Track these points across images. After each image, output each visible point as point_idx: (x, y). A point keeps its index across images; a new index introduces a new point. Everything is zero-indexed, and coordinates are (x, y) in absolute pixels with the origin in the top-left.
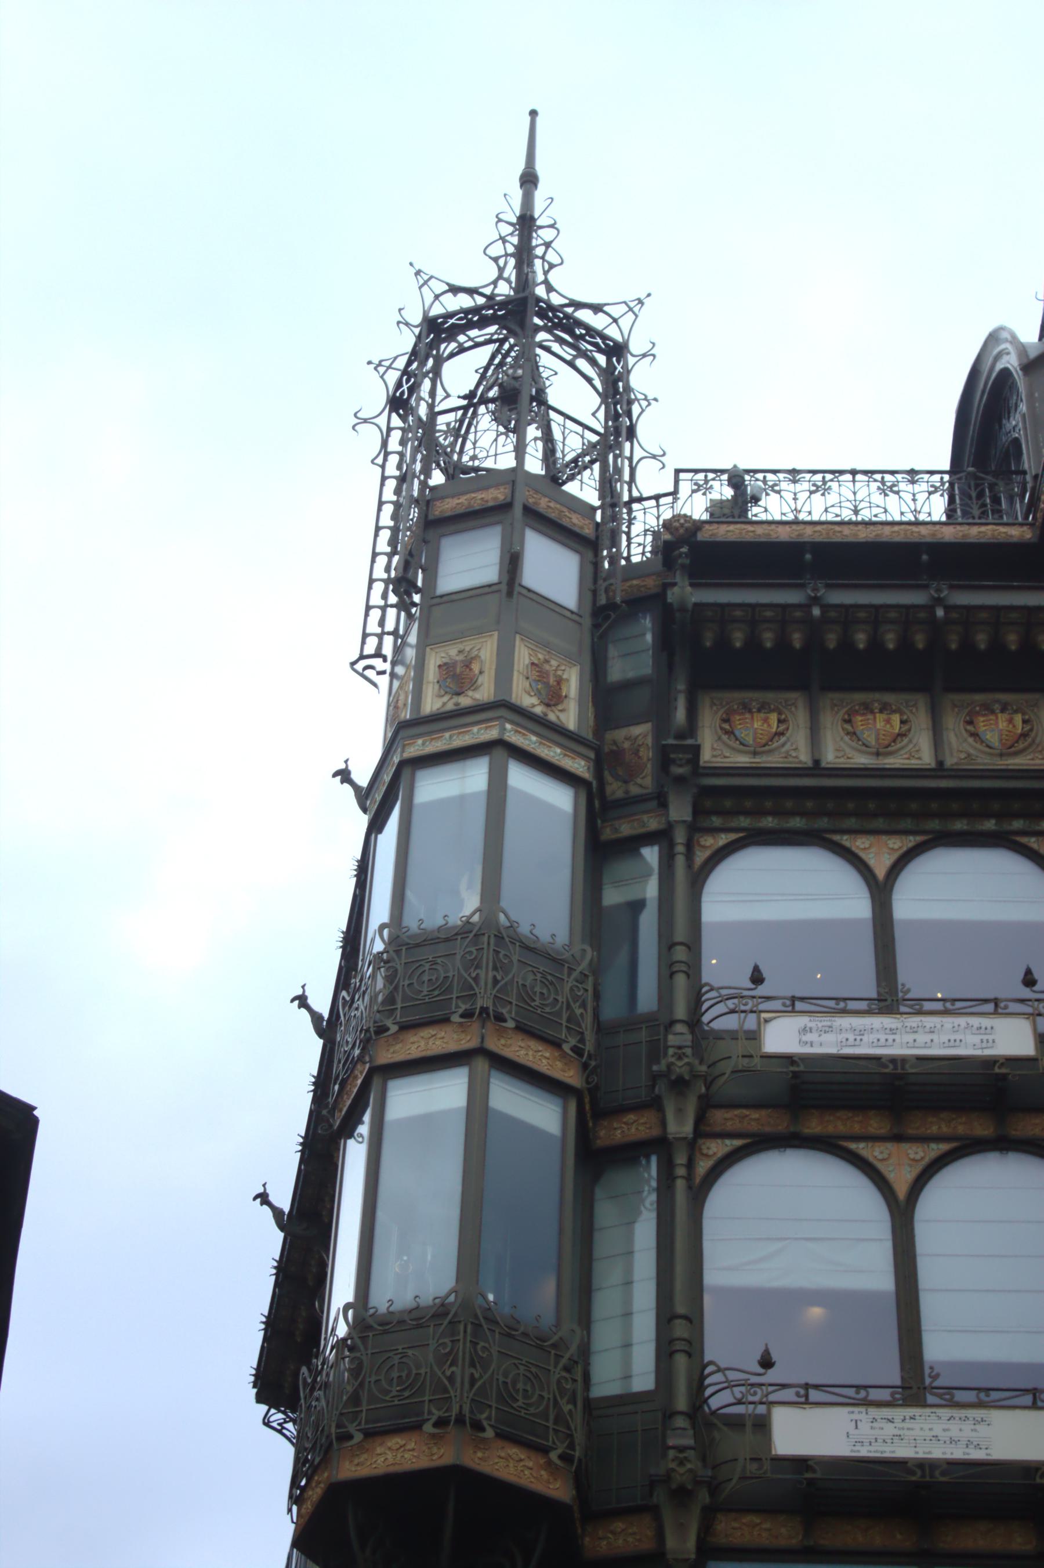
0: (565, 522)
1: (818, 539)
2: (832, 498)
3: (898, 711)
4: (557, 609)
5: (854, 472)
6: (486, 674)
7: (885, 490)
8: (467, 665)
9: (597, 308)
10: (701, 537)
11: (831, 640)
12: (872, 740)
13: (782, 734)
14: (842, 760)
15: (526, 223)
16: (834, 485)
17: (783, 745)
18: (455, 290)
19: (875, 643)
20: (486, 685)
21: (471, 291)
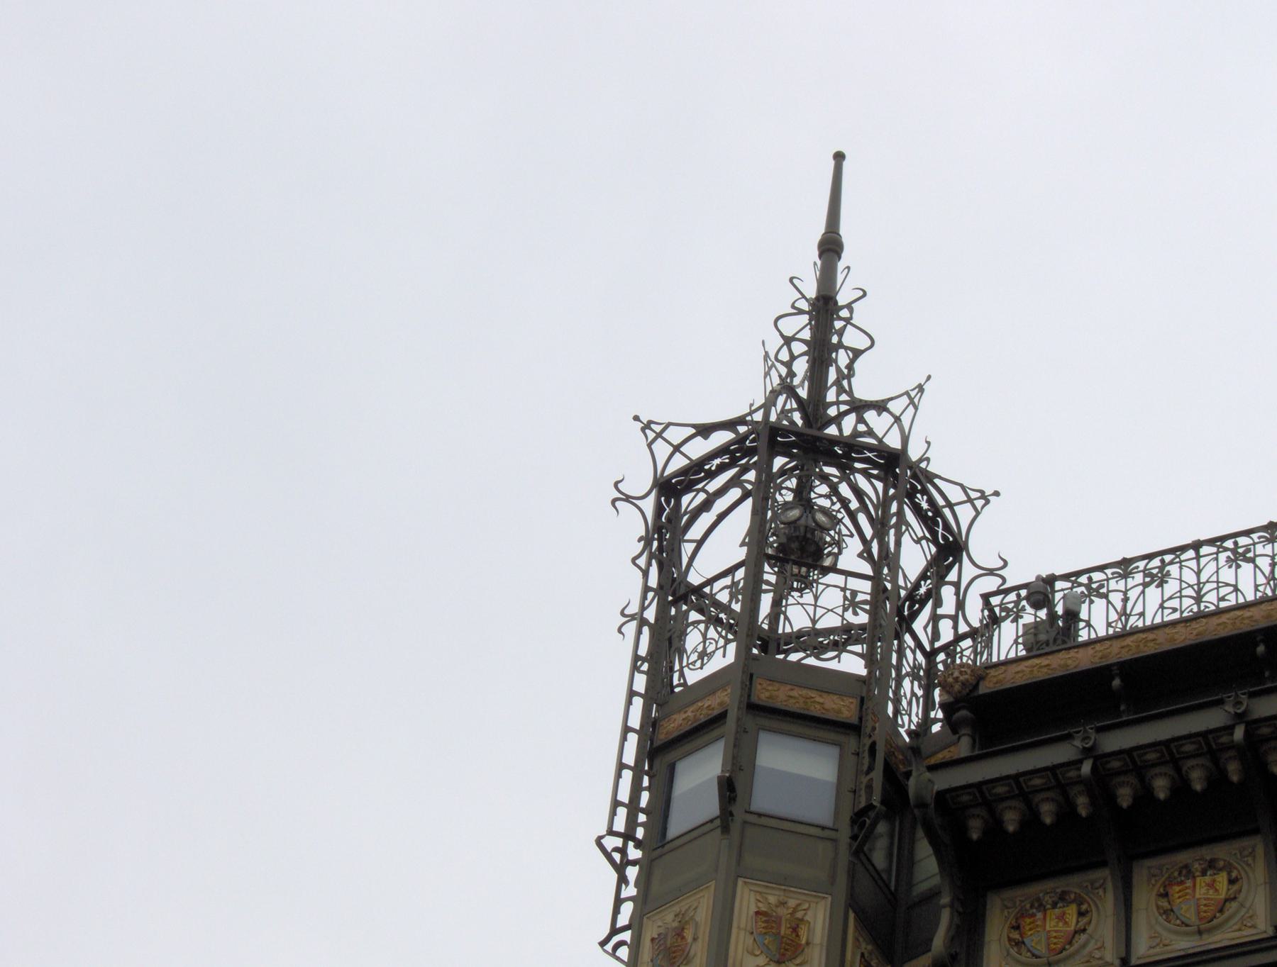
0: (815, 711)
1: (1126, 656)
2: (1171, 587)
3: (1228, 868)
4: (801, 829)
5: (1196, 546)
6: (700, 940)
7: (1239, 557)
8: (680, 933)
9: (880, 407)
10: (984, 689)
11: (1125, 796)
12: (1191, 917)
13: (1084, 930)
14: (1157, 950)
15: (824, 308)
16: (1174, 570)
17: (1084, 946)
18: (704, 430)
19: (1181, 787)
20: (699, 955)
21: (729, 425)
